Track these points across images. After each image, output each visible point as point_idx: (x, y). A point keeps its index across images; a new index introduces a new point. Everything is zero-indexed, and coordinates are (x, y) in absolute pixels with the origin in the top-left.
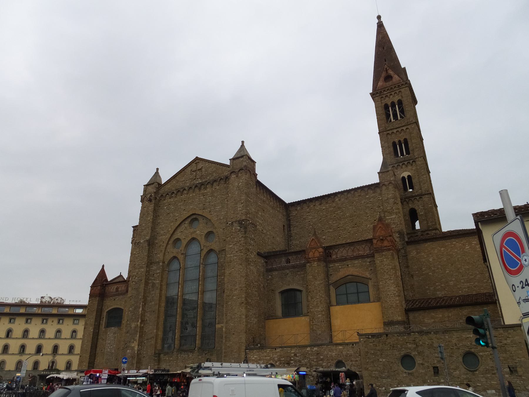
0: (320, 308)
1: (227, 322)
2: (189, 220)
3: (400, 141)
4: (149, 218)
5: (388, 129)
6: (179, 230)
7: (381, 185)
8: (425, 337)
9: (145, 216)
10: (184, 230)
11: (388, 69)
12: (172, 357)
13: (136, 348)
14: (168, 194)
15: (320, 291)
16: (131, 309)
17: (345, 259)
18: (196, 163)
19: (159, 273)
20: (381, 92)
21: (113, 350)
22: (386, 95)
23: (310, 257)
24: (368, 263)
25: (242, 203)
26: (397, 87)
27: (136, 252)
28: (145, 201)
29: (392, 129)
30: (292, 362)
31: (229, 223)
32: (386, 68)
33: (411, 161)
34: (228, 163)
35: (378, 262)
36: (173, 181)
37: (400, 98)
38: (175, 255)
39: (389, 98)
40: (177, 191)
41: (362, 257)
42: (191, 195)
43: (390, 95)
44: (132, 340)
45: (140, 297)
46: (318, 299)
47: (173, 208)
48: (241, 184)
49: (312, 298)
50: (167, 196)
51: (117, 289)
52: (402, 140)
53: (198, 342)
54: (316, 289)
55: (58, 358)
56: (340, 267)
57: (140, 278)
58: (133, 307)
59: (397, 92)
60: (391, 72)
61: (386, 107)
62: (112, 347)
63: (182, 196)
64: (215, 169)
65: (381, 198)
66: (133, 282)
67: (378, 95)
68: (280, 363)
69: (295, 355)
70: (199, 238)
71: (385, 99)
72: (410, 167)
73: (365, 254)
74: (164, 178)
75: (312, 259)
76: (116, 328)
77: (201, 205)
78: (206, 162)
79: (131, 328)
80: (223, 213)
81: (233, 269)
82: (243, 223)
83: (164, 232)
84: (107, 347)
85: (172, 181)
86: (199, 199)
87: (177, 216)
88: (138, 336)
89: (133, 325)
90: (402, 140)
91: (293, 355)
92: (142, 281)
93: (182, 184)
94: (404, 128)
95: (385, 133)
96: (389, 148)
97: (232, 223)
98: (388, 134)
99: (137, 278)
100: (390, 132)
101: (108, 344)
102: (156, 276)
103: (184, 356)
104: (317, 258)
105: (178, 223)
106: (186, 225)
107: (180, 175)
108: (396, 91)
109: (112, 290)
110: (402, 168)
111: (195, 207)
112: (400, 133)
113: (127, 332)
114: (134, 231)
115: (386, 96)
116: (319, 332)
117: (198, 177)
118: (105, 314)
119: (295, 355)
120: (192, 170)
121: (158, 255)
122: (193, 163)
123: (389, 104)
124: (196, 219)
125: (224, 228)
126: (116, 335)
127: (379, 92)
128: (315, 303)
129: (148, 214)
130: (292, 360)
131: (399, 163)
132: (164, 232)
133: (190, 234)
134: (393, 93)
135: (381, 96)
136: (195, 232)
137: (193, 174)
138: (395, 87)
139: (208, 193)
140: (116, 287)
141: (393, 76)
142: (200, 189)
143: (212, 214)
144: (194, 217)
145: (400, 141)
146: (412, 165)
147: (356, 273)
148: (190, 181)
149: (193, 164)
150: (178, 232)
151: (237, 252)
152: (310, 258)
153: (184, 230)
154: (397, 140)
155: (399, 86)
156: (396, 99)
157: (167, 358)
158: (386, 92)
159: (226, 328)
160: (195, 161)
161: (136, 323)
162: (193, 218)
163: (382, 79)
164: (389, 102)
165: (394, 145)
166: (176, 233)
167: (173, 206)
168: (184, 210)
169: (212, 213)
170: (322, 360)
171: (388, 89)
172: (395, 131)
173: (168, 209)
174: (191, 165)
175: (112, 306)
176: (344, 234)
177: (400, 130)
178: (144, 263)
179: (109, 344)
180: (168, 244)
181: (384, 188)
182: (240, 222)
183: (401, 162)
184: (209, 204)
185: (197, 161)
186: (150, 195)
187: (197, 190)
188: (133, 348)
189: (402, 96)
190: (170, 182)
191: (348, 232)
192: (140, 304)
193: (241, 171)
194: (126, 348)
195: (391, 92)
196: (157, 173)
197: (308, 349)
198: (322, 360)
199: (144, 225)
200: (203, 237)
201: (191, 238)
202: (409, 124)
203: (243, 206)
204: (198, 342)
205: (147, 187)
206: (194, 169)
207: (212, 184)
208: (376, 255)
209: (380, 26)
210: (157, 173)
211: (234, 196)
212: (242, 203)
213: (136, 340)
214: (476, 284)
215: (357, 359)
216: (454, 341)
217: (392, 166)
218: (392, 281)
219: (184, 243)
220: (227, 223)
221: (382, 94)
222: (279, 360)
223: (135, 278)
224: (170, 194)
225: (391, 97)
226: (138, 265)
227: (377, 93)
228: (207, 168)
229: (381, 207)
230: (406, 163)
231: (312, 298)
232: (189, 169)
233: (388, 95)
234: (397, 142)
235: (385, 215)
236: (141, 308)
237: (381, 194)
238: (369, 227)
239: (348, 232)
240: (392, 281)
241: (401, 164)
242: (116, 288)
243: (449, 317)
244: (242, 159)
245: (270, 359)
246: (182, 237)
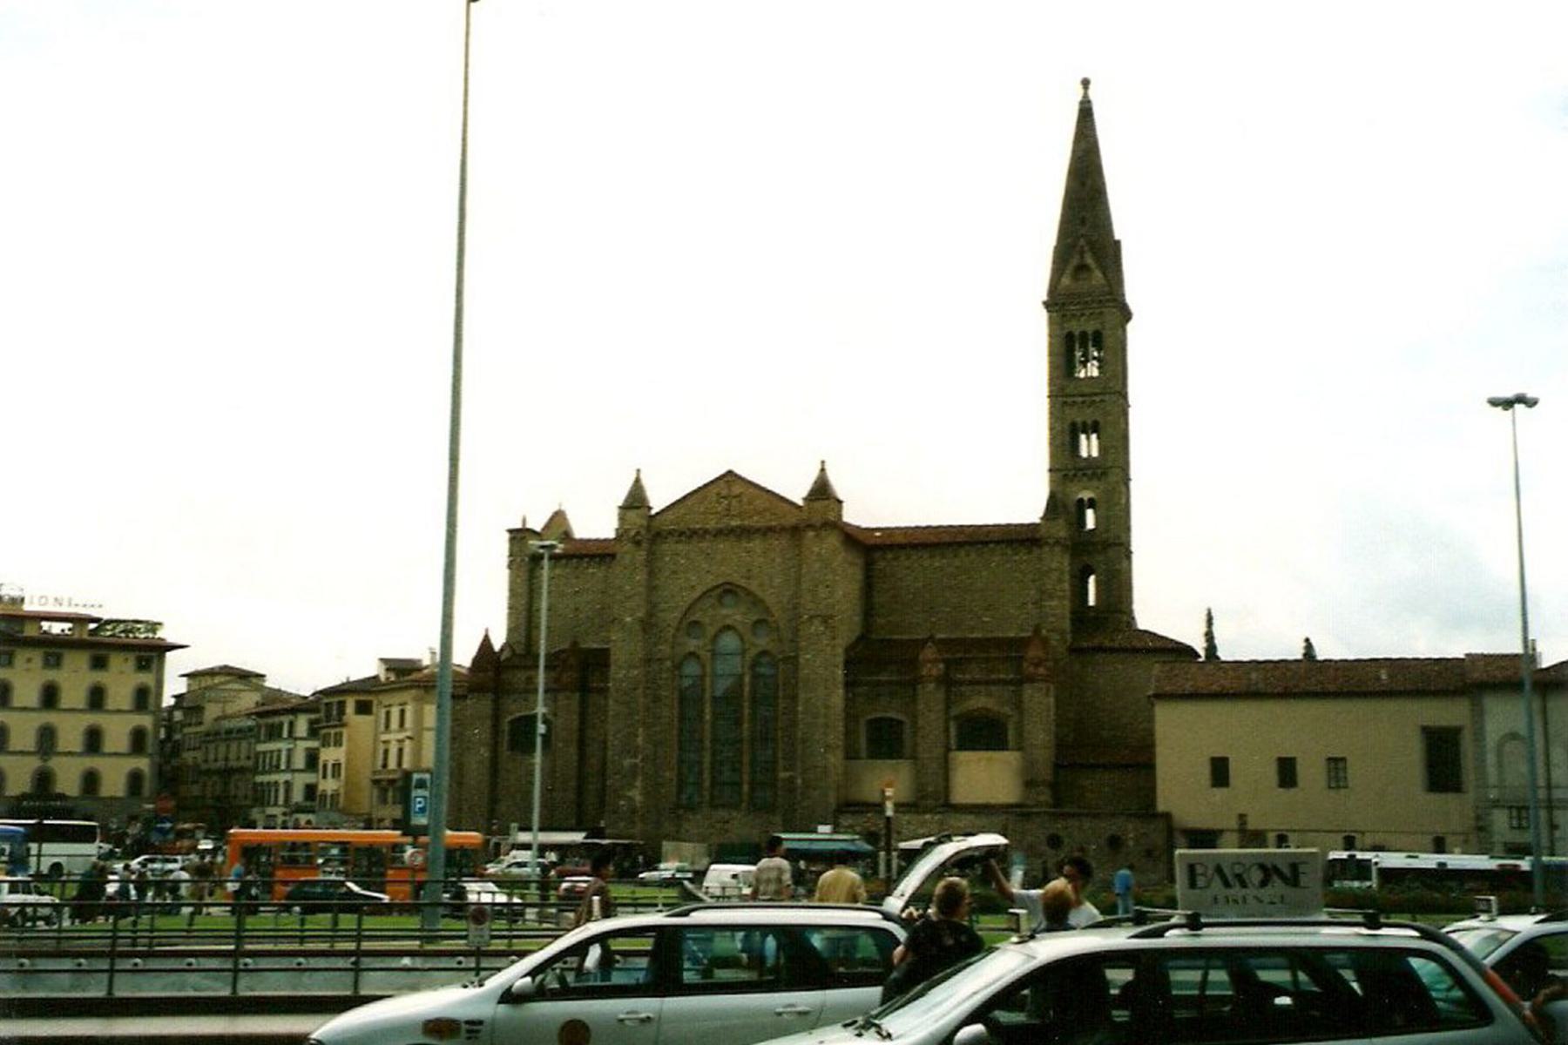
34: (801, 503)
37: (1099, 327)
55: (55, 763)
60: (1089, 260)
61: (1070, 337)
64: (767, 504)
69: (909, 823)
72: (1095, 483)
74: (659, 499)
94: (1097, 399)
98: (1065, 403)
105: (696, 594)
114: (512, 540)
118: (506, 727)
144: (728, 587)
156: (1090, 328)
159: (803, 779)
163: (1069, 270)
164: (1076, 327)
172: (1080, 399)
185: (729, 478)
187: (732, 538)
188: (631, 799)
206: (724, 493)
209: (1086, 113)
210: (638, 481)
219: (711, 631)
225: (1083, 319)
230: (1089, 472)
237: (1040, 559)
241: (1080, 473)
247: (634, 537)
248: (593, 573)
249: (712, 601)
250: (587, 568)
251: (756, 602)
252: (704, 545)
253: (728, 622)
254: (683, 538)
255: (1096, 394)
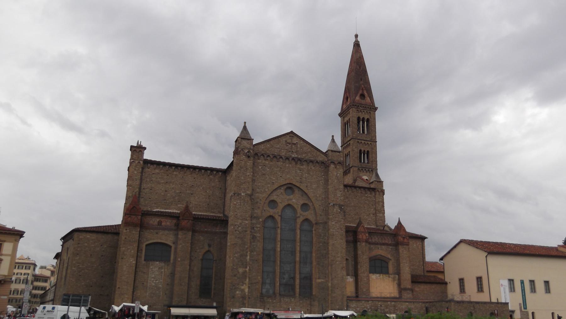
0: (366, 274)
1: (332, 280)
2: (285, 187)
3: (364, 151)
4: (248, 174)
5: (358, 138)
6: (275, 193)
7: (376, 190)
8: (477, 305)
9: (243, 169)
10: (280, 194)
11: (364, 89)
12: (275, 300)
13: (247, 290)
14: (262, 155)
15: (366, 263)
16: (236, 255)
17: (377, 244)
18: (290, 136)
19: (260, 227)
20: (358, 106)
21: (160, 285)
22: (361, 110)
23: (360, 238)
24: (390, 249)
25: (340, 191)
26: (369, 108)
27: (237, 203)
28: (242, 155)
29: (361, 140)
30: (379, 310)
31: (331, 204)
32: (363, 88)
33: (370, 170)
35: (401, 251)
36: (267, 144)
37: (368, 117)
38: (272, 214)
39: (362, 113)
40: (273, 156)
41: (387, 245)
42: (287, 165)
43: (364, 111)
44: (241, 284)
45: (246, 246)
46: (364, 268)
47: (268, 171)
48: (338, 175)
49: (361, 267)
50: (262, 156)
51: (160, 223)
52: (366, 151)
53: (297, 290)
54: (364, 261)
56: (374, 248)
57: (244, 229)
58: (239, 254)
59: (368, 112)
62: (157, 281)
63: (278, 162)
64: (309, 150)
65: (374, 199)
66: (236, 230)
67: (355, 107)
68: (371, 310)
69: (381, 306)
70: (295, 206)
71: (359, 113)
72: (368, 173)
73: (389, 243)
75: (361, 240)
76: (162, 263)
77: (298, 178)
78: (301, 140)
79: (238, 272)
80: (318, 192)
81: (336, 241)
82: (343, 208)
83: (261, 190)
84: (150, 280)
85: (266, 143)
86: (296, 172)
87: (274, 180)
88: (247, 280)
89: (241, 270)
90: (366, 151)
91: (379, 306)
92: (247, 233)
93: (277, 151)
95: (356, 140)
96: (358, 153)
97: (334, 205)
99: (240, 228)
100: (360, 141)
101: (152, 278)
102: (257, 230)
103: (287, 300)
104: (364, 240)
106: (282, 191)
107: (273, 141)
108: (368, 111)
109: (151, 222)
110: (363, 172)
111: (292, 178)
112: (366, 145)
113: (235, 276)
115: (361, 111)
116: (364, 290)
117: (293, 151)
118: (144, 246)
119: (381, 306)
120: (286, 141)
121: (256, 211)
122: (288, 134)
123: (361, 118)
124: (290, 188)
125: (321, 205)
126: (163, 270)
127: (357, 105)
128: (363, 271)
129: (247, 169)
130: (379, 309)
131: (363, 168)
132: (261, 191)
133: (286, 200)
134: (365, 111)
135: (357, 109)
136: (291, 199)
137: (288, 145)
138: (368, 108)
139: (305, 170)
140: (158, 220)
141: (367, 98)
142: (296, 163)
143: (308, 190)
144: (290, 186)
145: (364, 151)
146: (370, 172)
147: (383, 254)
148: (286, 151)
149: (287, 135)
150: (274, 195)
151: (338, 229)
152: (360, 239)
153: (280, 194)
154: (363, 150)
155: (371, 108)
156: (366, 117)
157: (271, 301)
158: (362, 108)
159: (331, 283)
160: (289, 134)
161: (244, 269)
162: (290, 188)
163: (359, 95)
165: (360, 151)
166: (271, 195)
167: (269, 169)
168: (281, 176)
169: (309, 189)
170: (397, 310)
171: (363, 107)
172: (363, 142)
173: (263, 170)
174: (285, 136)
175: (154, 239)
176: (349, 218)
177: (366, 142)
178: (247, 216)
179: (154, 278)
180: (265, 203)
181: (378, 193)
182: (340, 207)
183: (364, 168)
184: (306, 180)
185: (291, 135)
186: (248, 150)
188: (243, 291)
189: (370, 117)
190: (264, 144)
191: (352, 218)
192: (247, 252)
193: (339, 165)
194: (235, 289)
195: (364, 110)
196: (245, 127)
197: (389, 303)
198: (397, 310)
199: (242, 178)
200: (300, 207)
201: (287, 204)
202: (372, 140)
203: (341, 194)
204: (297, 290)
205: (242, 140)
206: (289, 141)
207: (308, 163)
208: (400, 247)
209: (357, 45)
210: (245, 127)
211: (334, 183)
212: (340, 191)
213: (245, 284)
214: (416, 268)
215: (416, 311)
216: (488, 308)
217: (358, 168)
218: (407, 265)
219: (281, 206)
220: (330, 204)
221: (358, 108)
222: (371, 308)
223: (238, 228)
224: (266, 156)
225: (363, 113)
226: (240, 216)
227: (356, 105)
228: (302, 146)
229: (374, 206)
231: (361, 267)
232: (284, 139)
233: (362, 111)
234: (363, 151)
235: (376, 212)
236: (249, 256)
237: (375, 197)
238: (365, 218)
239: (352, 218)
240: (407, 265)
241: (364, 169)
242: (159, 221)
243: (426, 288)
244: (338, 154)
245: (365, 308)
246: (278, 200)
247: (247, 153)
248: (176, 175)
249: (282, 191)
250: (174, 171)
251: (304, 193)
252: (280, 164)
253: (290, 202)
254: (268, 158)
255: (366, 141)
